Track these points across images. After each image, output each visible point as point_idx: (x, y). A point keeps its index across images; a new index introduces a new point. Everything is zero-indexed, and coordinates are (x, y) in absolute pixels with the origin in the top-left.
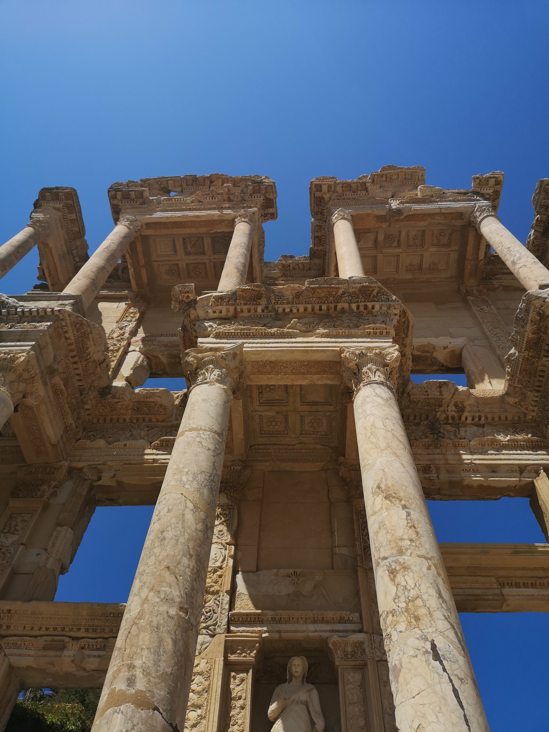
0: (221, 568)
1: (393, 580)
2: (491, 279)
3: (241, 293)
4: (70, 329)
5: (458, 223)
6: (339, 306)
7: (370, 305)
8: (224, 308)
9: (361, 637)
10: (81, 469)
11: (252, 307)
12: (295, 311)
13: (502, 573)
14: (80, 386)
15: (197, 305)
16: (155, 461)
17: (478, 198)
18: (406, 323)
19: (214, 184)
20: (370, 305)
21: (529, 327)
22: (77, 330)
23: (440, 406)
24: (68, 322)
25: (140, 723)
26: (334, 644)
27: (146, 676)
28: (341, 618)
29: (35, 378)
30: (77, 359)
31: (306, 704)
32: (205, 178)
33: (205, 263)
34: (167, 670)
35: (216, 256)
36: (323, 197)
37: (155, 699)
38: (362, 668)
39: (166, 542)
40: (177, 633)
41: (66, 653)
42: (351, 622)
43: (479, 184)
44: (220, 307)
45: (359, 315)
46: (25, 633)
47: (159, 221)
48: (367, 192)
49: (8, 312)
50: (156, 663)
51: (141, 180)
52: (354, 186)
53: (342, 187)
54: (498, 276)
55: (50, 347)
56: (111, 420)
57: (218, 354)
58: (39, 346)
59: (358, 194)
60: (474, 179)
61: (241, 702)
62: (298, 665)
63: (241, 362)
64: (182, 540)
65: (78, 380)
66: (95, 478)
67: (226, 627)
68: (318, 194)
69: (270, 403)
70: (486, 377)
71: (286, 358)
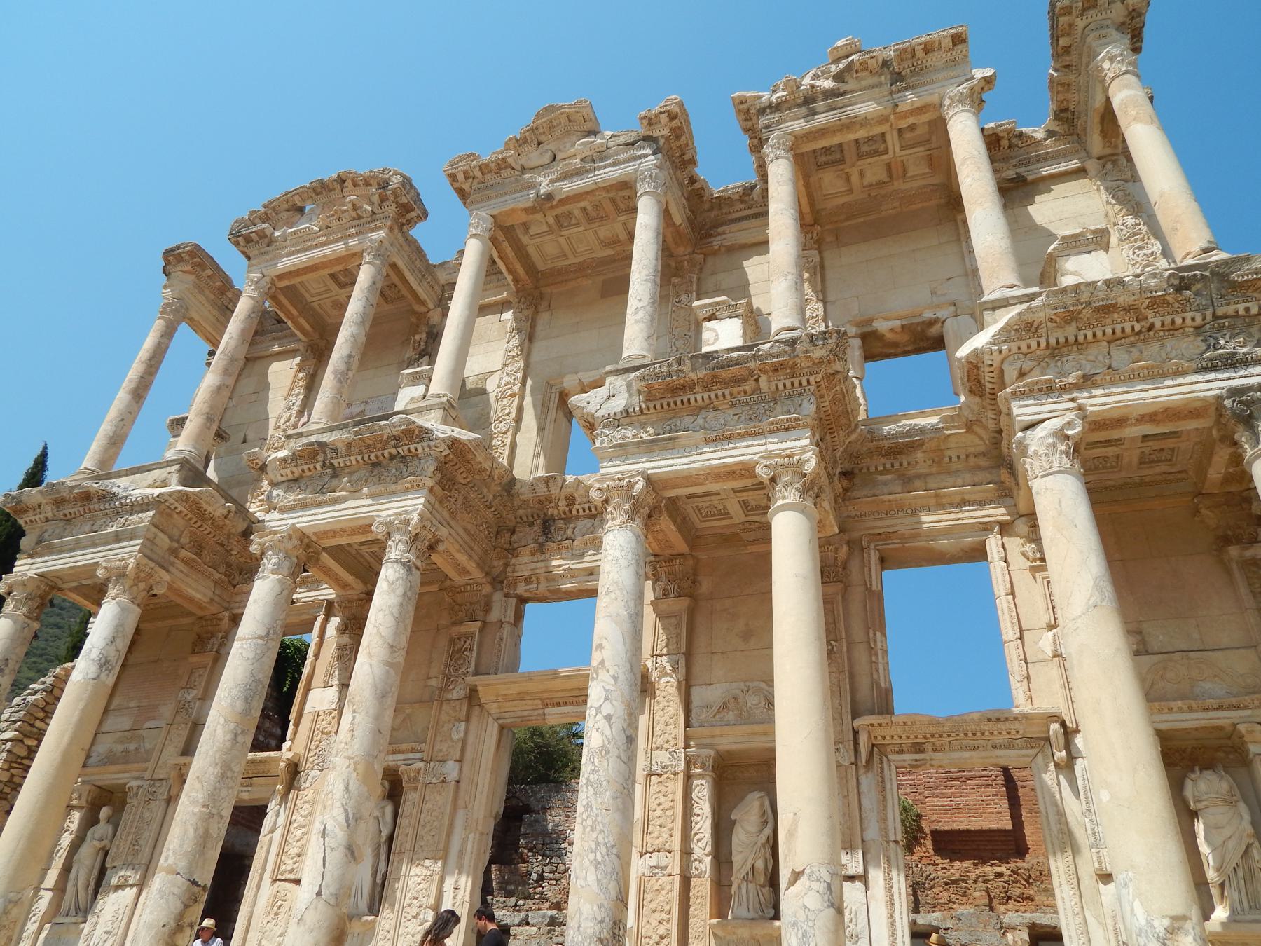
2: (711, 236)
4: (176, 505)
7: (412, 447)
8: (288, 471)
13: (545, 695)
17: (644, 152)
20: (412, 447)
23: (551, 502)
43: (650, 124)
50: (181, 846)
51: (264, 206)
52: (493, 166)
54: (720, 230)
55: (161, 535)
60: (641, 119)
64: (211, 753)
68: (457, 185)
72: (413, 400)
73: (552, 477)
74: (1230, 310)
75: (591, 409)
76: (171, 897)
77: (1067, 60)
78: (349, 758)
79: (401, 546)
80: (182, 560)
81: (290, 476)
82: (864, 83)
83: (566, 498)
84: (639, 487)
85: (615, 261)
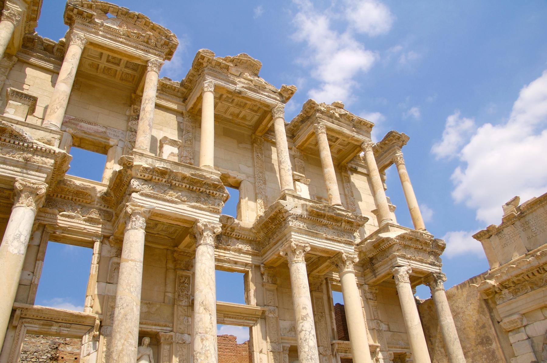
1: (202, 342)
5: (266, 109)
6: (202, 189)
8: (147, 175)
9: (172, 333)
10: (44, 226)
11: (161, 179)
12: (180, 186)
13: (226, 313)
15: (133, 169)
16: (85, 229)
19: (140, 20)
20: (215, 192)
21: (273, 213)
26: (162, 335)
31: (149, 356)
32: (134, 15)
33: (117, 71)
35: (126, 69)
38: (171, 344)
41: (52, 328)
42: (168, 327)
44: (145, 174)
45: (208, 195)
46: (34, 318)
47: (100, 44)
49: (28, 146)
52: (222, 65)
56: (61, 196)
57: (143, 209)
66: (52, 232)
68: (201, 61)
70: (247, 198)
72: (172, 154)
73: (231, 218)
74: (434, 250)
75: (288, 208)
77: (383, 146)
78: (214, 336)
79: (211, 238)
81: (144, 178)
82: (347, 122)
83: (231, 228)
84: (309, 249)
85: (239, 125)
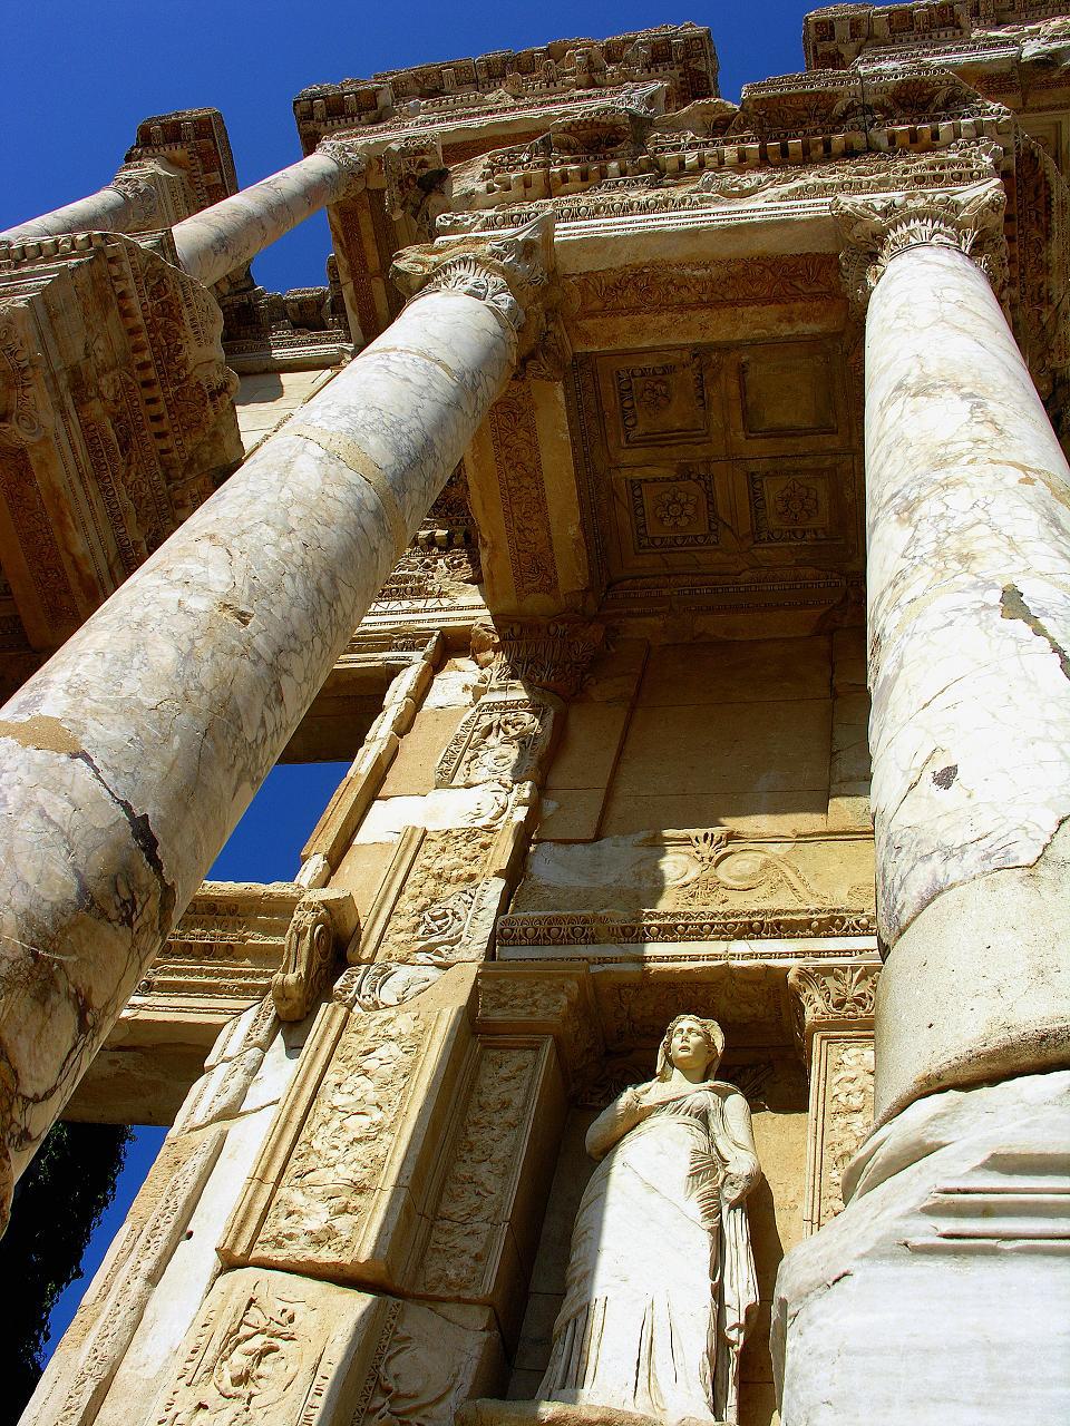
0: (489, 829)
3: (564, 137)
4: (130, 286)
14: (163, 452)
18: (1042, 191)
22: (152, 294)
24: (126, 266)
25: (22, 768)
26: (804, 975)
27: (74, 695)
28: (832, 919)
29: (30, 373)
30: (152, 373)
31: (703, 1117)
34: (144, 698)
36: (839, 53)
37: (84, 737)
39: (223, 503)
40: (199, 643)
48: (959, 27)
53: (890, 21)
58: (45, 303)
59: (935, 35)
61: (510, 1115)
62: (687, 1033)
63: (554, 274)
65: (161, 435)
67: (485, 946)
68: (829, 47)
69: (660, 439)
71: (676, 254)
76: (29, 822)
80: (85, 426)
